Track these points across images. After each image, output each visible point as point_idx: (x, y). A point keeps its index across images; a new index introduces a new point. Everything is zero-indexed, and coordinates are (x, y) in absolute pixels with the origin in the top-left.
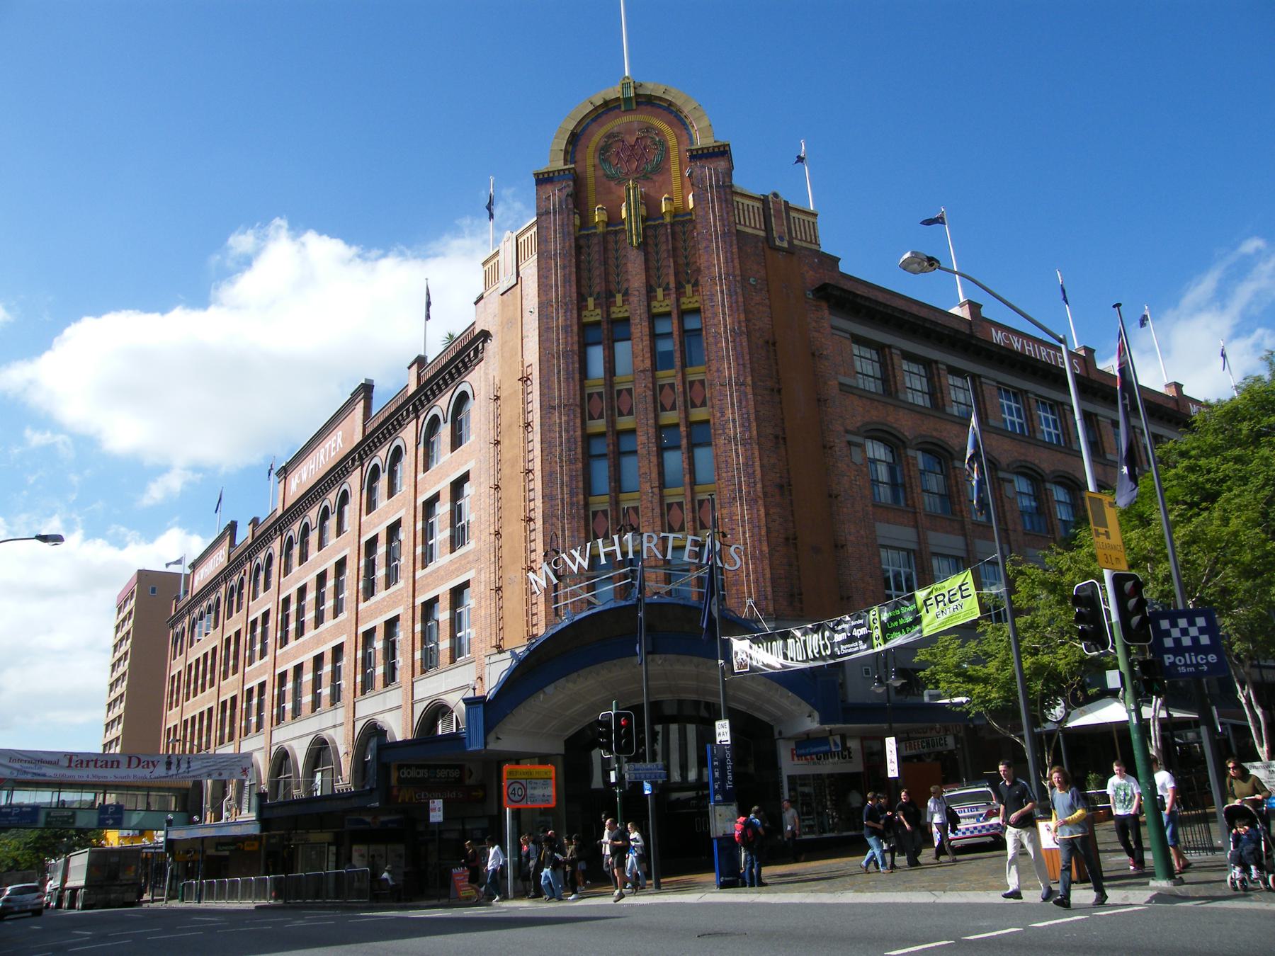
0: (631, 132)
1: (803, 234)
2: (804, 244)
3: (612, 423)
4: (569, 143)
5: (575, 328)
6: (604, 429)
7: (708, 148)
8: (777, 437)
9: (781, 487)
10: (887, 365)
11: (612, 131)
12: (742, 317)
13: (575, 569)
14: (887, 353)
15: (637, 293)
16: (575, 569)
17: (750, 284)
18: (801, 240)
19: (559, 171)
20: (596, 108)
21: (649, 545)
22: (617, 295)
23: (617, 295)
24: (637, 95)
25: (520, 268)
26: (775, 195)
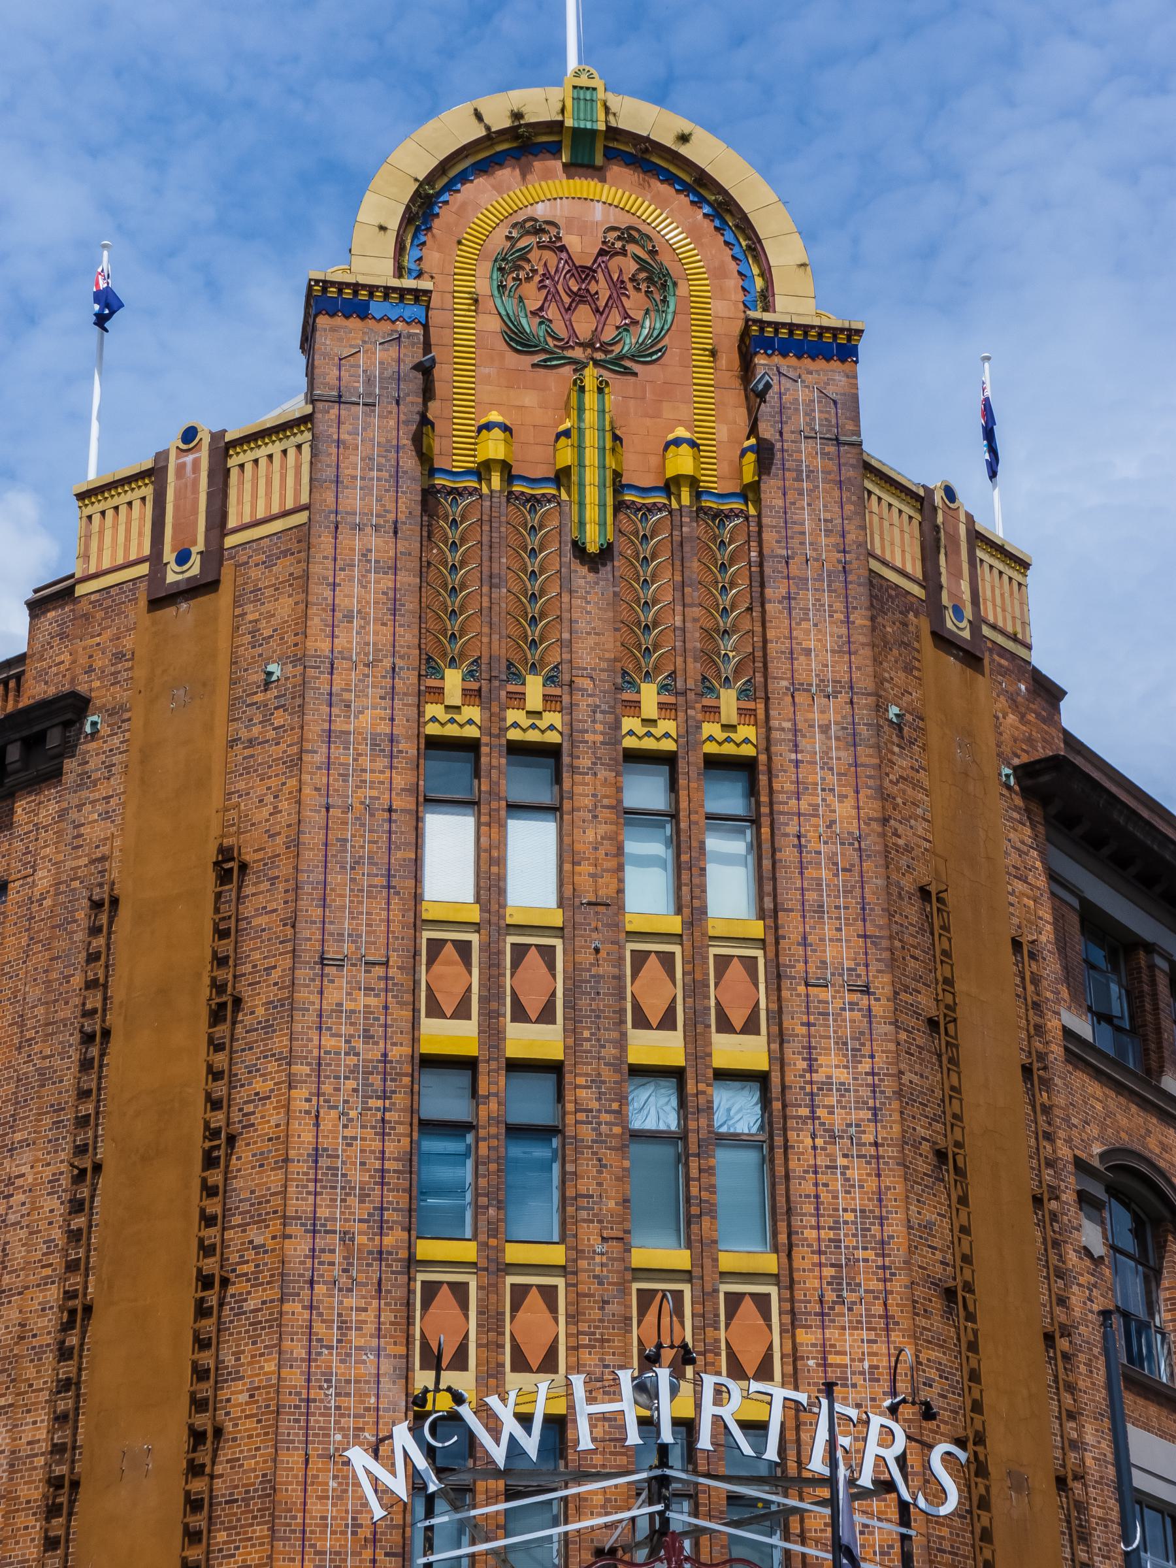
0: (583, 229)
1: (999, 610)
2: (1000, 640)
3: (492, 1034)
4: (409, 219)
5: (409, 748)
6: (472, 1050)
7: (806, 328)
8: (941, 1155)
9: (950, 1294)
10: (1141, 996)
11: (529, 212)
12: (872, 808)
13: (499, 1454)
14: (1143, 964)
15: (586, 683)
16: (499, 1454)
17: (891, 721)
18: (994, 627)
19: (387, 291)
20: (491, 137)
21: (718, 1411)
22: (530, 679)
23: (530, 679)
24: (609, 129)
25: (230, 541)
26: (950, 493)
